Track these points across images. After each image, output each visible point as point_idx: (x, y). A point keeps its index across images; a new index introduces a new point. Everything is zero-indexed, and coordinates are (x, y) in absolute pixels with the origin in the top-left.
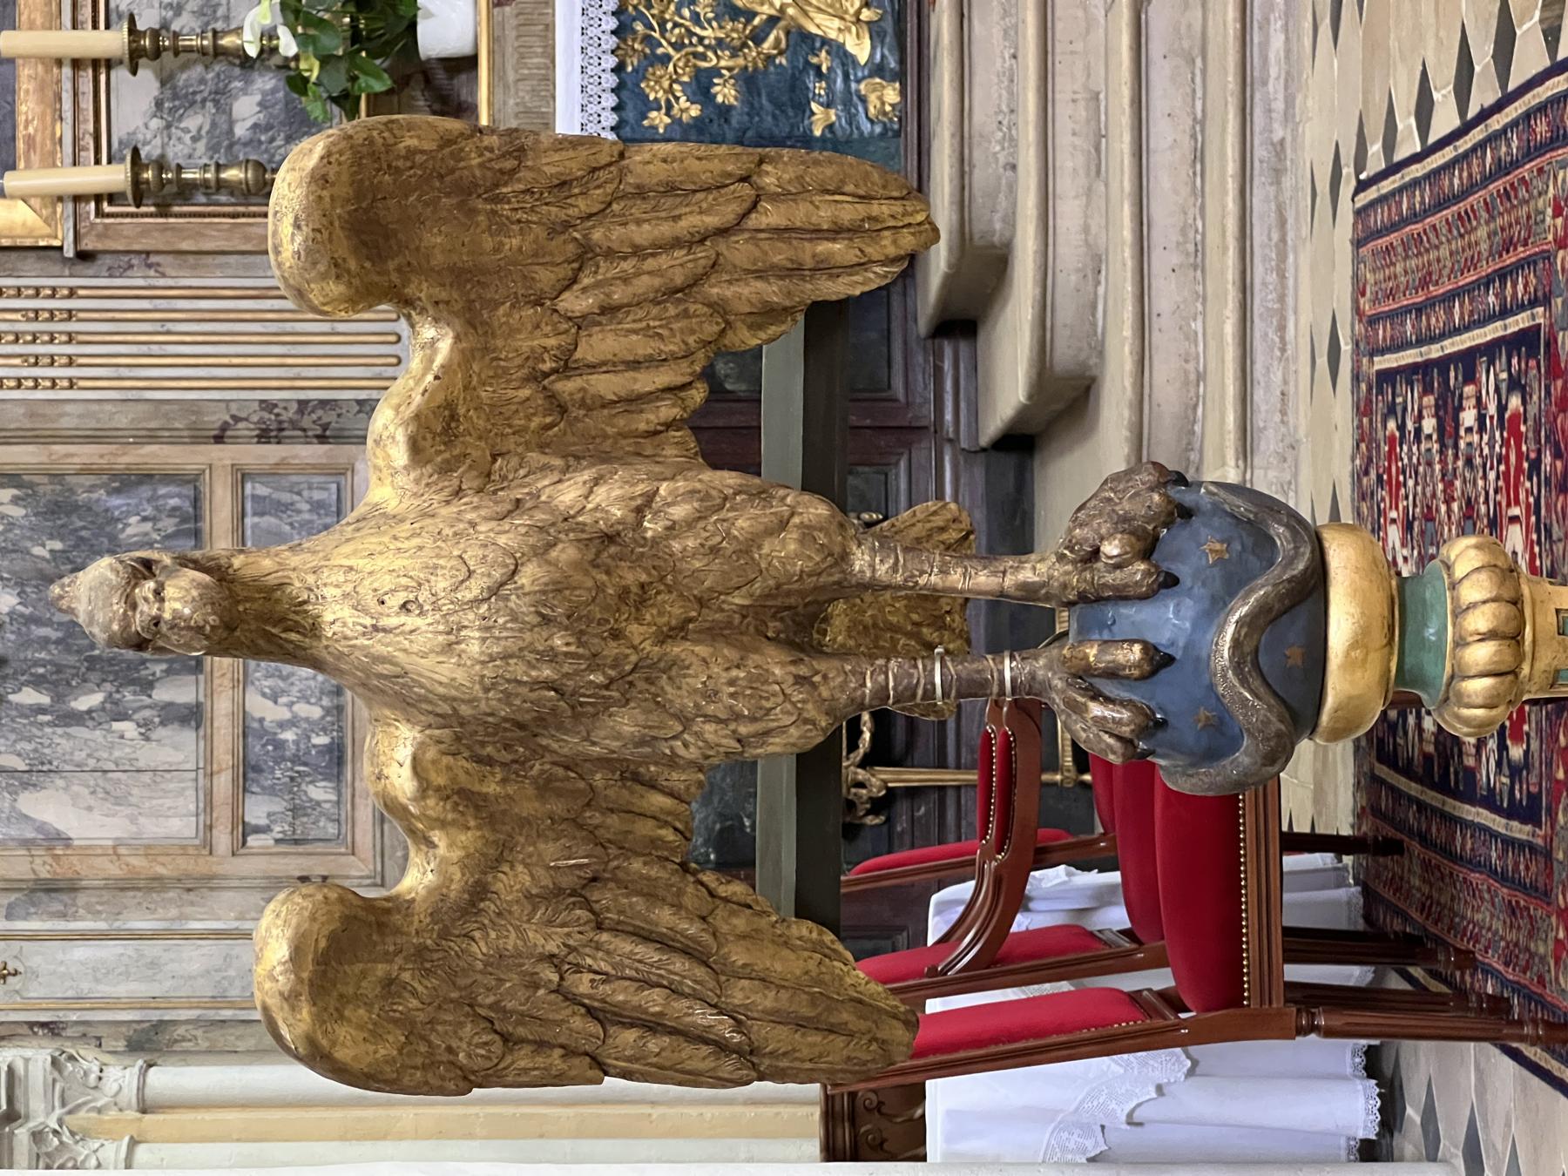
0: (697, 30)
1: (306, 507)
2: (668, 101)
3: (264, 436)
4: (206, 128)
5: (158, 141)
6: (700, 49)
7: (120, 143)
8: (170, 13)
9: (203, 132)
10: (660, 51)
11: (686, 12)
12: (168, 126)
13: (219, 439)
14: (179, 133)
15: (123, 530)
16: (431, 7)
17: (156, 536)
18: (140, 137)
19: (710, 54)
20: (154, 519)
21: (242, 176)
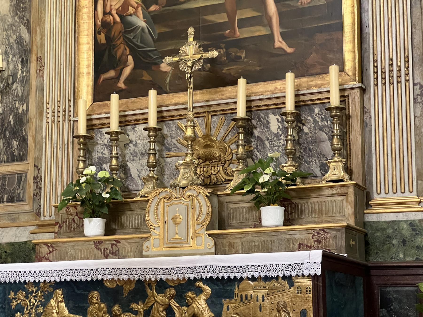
0: (34, 308)
1: (19, 191)
2: (16, 298)
3: (35, 178)
4: (105, 156)
5: (102, 142)
6: (29, 308)
7: (101, 131)
8: (134, 143)
9: (104, 155)
10: (29, 295)
11: (39, 303)
12: (105, 145)
13: (35, 166)
14: (103, 148)
15: (15, 140)
16: (92, 223)
17: (13, 149)
18: (103, 137)
19: (28, 312)
20: (17, 149)
21: (80, 168)
